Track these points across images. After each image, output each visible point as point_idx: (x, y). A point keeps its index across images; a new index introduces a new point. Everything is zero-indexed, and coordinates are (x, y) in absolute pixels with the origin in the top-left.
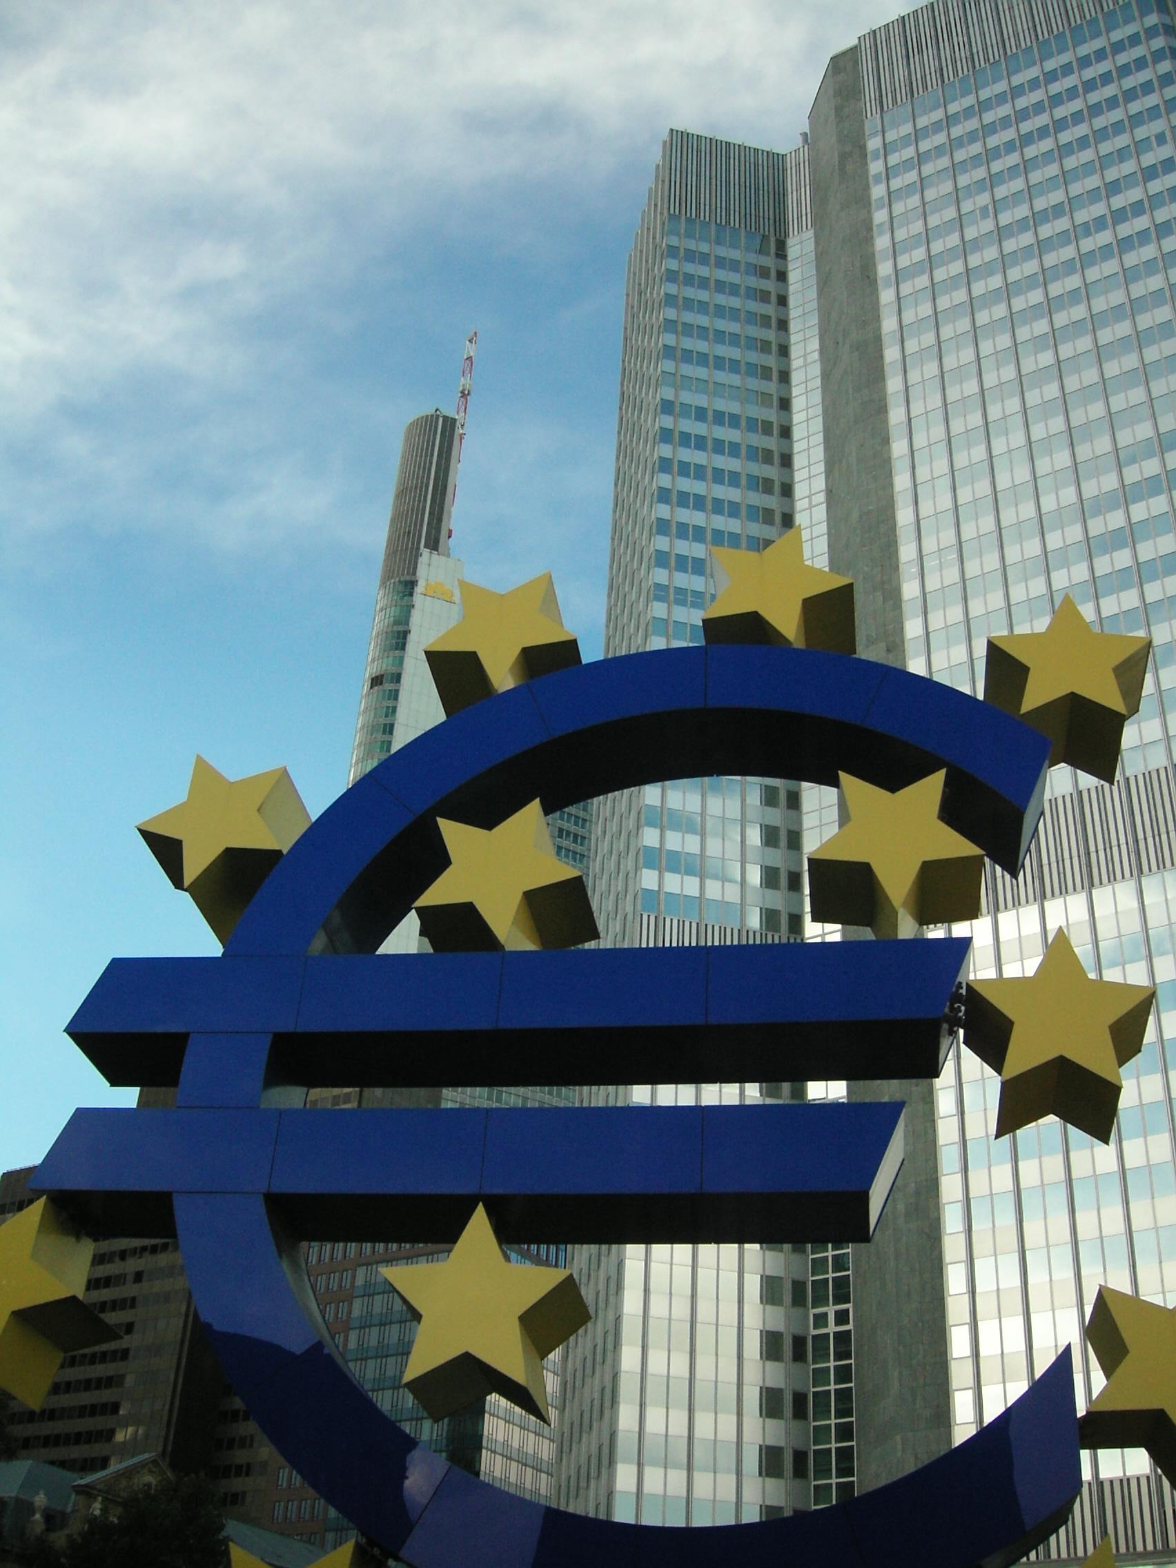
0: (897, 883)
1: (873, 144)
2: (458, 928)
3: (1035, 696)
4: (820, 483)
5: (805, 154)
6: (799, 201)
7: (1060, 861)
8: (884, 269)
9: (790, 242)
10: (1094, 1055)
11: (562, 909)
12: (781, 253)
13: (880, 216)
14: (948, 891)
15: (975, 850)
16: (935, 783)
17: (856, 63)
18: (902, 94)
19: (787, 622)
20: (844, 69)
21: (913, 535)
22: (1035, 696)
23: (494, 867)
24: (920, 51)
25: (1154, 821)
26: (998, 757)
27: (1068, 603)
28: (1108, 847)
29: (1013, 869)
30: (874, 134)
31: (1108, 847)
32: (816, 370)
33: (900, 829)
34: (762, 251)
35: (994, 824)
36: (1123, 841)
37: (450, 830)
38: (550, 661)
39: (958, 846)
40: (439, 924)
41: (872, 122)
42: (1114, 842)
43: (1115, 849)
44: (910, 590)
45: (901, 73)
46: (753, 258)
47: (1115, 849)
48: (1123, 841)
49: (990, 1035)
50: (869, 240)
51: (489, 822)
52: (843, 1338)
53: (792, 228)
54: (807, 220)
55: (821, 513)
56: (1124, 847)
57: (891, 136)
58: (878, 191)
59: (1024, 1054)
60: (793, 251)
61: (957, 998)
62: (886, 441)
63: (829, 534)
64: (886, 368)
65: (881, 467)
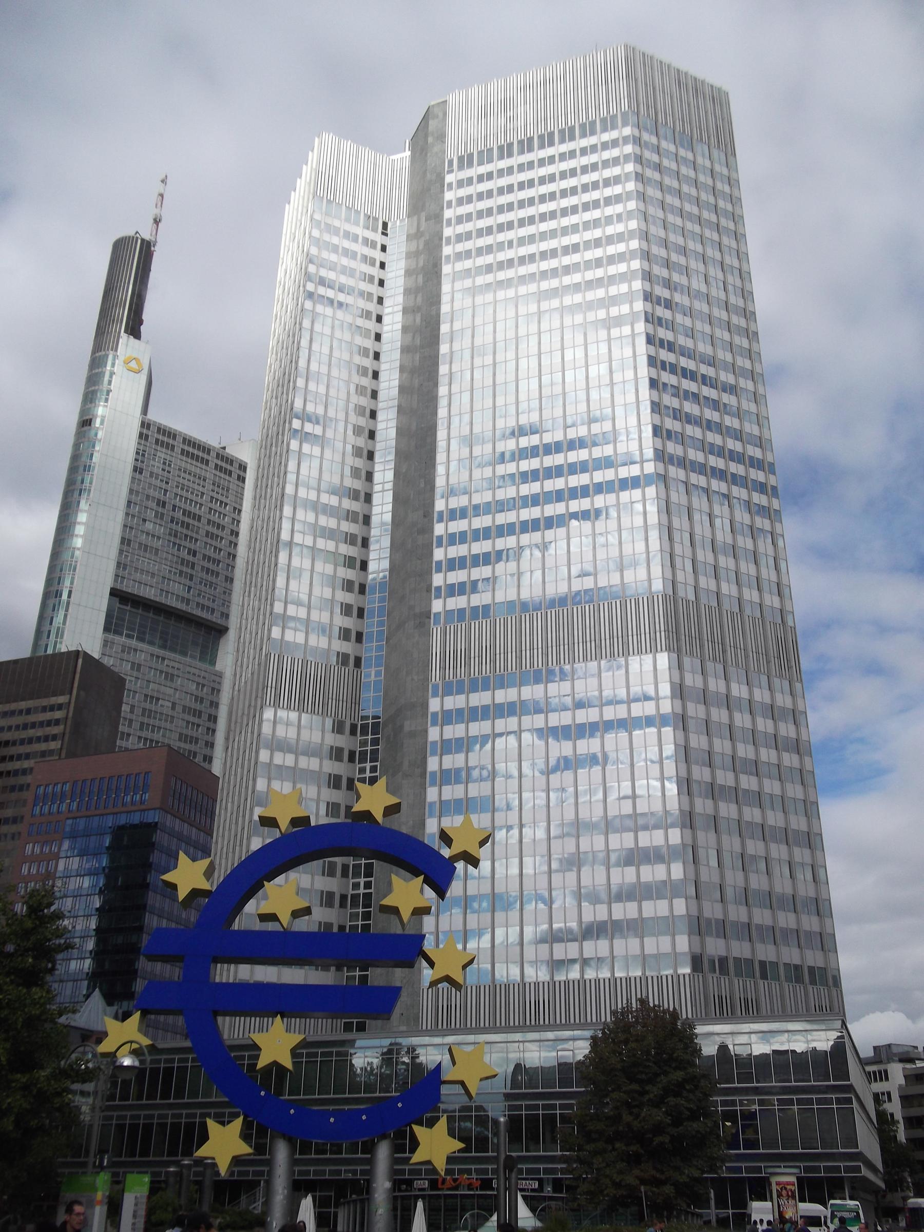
1: (449, 178)
19: (378, 816)
36: (540, 646)
42: (535, 647)
43: (535, 651)
47: (535, 651)
48: (540, 646)
52: (368, 896)
56: (540, 650)
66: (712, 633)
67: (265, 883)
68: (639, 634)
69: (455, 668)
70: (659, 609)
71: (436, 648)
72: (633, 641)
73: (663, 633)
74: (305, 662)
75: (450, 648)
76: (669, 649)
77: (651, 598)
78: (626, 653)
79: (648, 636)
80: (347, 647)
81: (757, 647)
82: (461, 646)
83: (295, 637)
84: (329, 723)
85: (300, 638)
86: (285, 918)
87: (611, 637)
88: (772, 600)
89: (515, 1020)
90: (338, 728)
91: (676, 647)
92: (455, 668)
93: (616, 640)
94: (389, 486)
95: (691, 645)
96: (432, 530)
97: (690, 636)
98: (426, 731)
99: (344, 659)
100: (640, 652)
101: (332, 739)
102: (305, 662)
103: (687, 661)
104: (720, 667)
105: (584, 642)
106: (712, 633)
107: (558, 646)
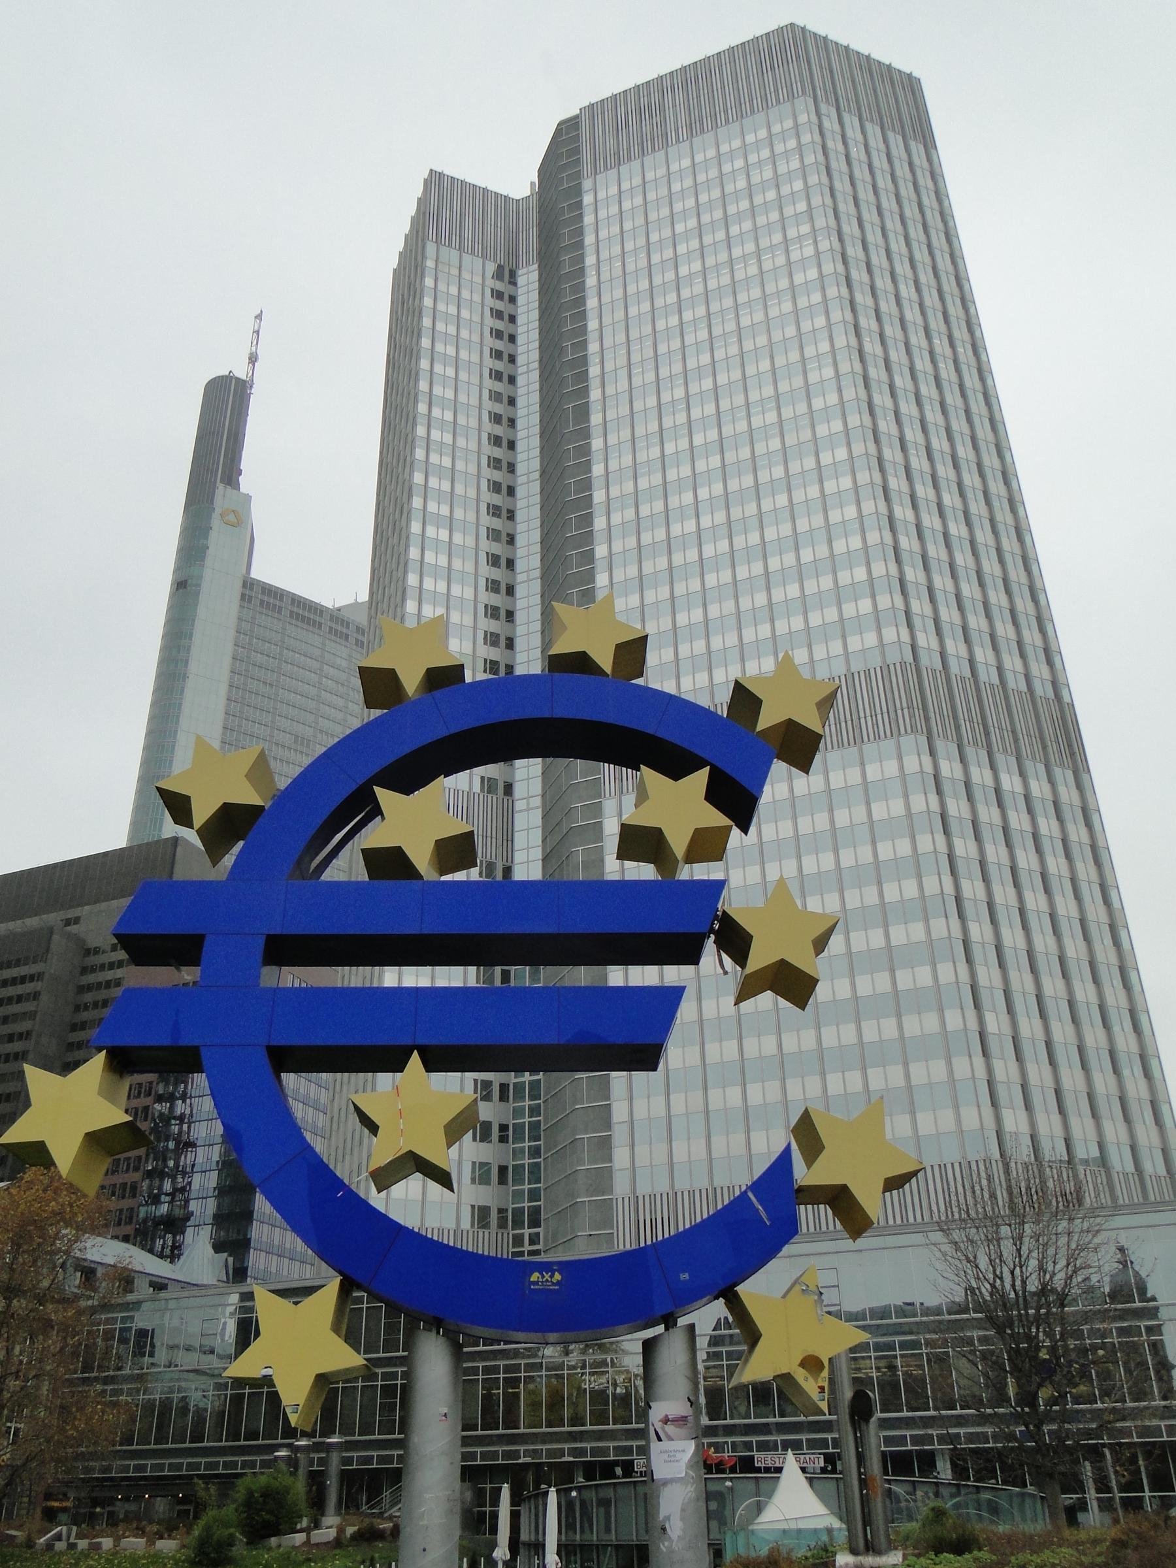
0: (679, 844)
1: (588, 199)
2: (389, 864)
3: (767, 719)
4: (536, 464)
5: (534, 203)
9: (520, 272)
10: (802, 959)
11: (456, 850)
14: (708, 845)
15: (724, 821)
16: (703, 775)
19: (605, 660)
22: (767, 719)
23: (411, 822)
26: (734, 755)
27: (788, 659)
29: (745, 829)
33: (679, 805)
35: (736, 801)
37: (381, 793)
38: (443, 678)
39: (716, 818)
40: (370, 856)
45: (611, 143)
49: (735, 941)
51: (408, 790)
53: (523, 259)
55: (536, 487)
59: (758, 959)
60: (521, 281)
61: (716, 917)
66: (969, 710)
67: (383, 795)
72: (867, 724)
73: (906, 711)
77: (886, 669)
79: (886, 715)
86: (421, 858)
88: (1039, 670)
93: (843, 724)
95: (944, 725)
97: (942, 715)
98: (602, 860)
100: (877, 737)
103: (940, 744)
104: (983, 754)
106: (969, 710)
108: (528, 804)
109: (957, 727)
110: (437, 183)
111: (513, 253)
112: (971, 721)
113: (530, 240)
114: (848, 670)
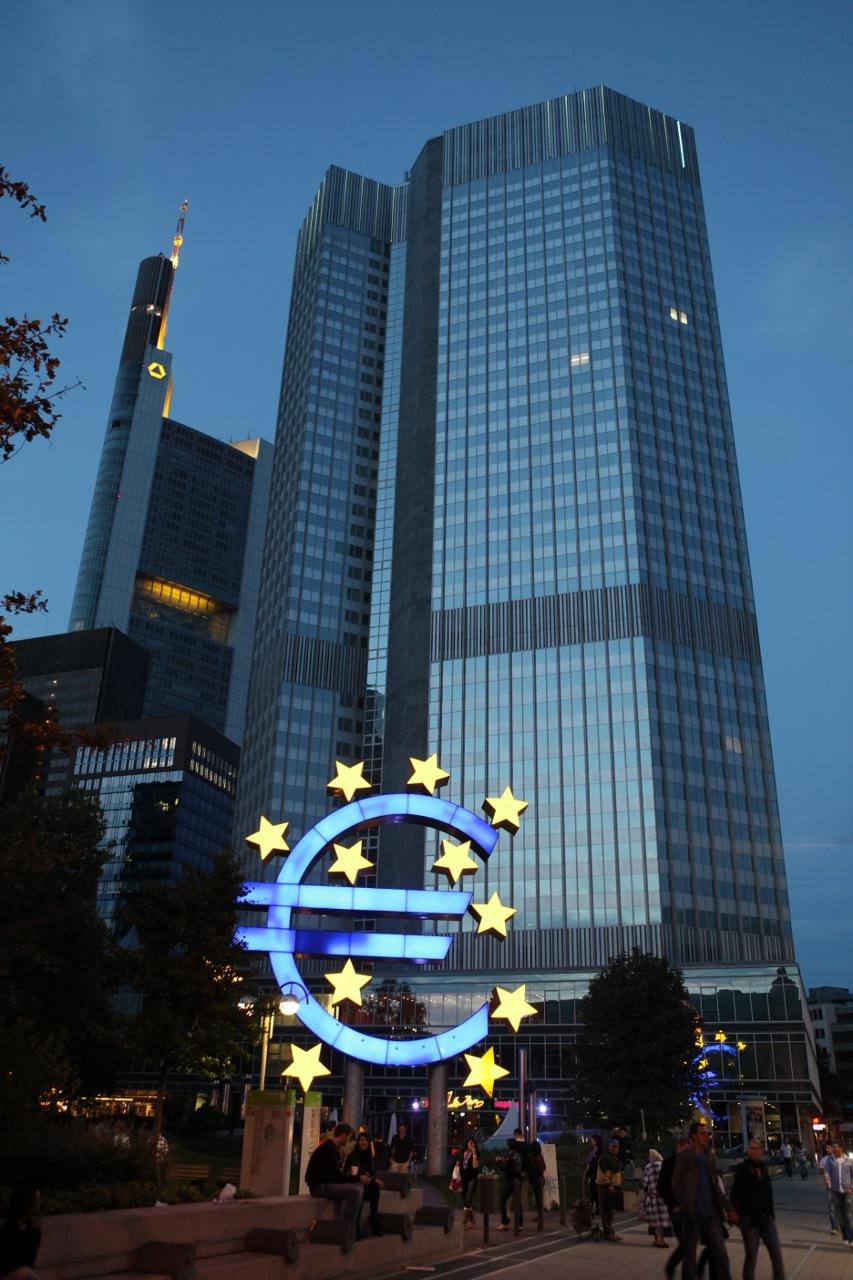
1: (446, 205)
4: (397, 400)
5: (406, 192)
6: (399, 223)
7: (498, 635)
8: (444, 287)
9: (393, 247)
12: (387, 254)
13: (445, 254)
17: (441, 148)
18: (465, 177)
20: (434, 147)
21: (443, 449)
24: (478, 151)
25: (545, 624)
28: (522, 632)
30: (446, 199)
31: (522, 632)
32: (400, 330)
34: (378, 252)
41: (446, 193)
44: (439, 479)
45: (465, 163)
46: (371, 255)
50: (437, 268)
54: (403, 234)
55: (395, 417)
57: (456, 203)
58: (445, 237)
60: (394, 254)
62: (434, 392)
63: (399, 429)
64: (439, 348)
65: (430, 407)
68: (618, 619)
69: (453, 648)
70: (636, 597)
71: (436, 631)
72: (613, 626)
73: (639, 620)
74: (318, 642)
75: (448, 630)
76: (645, 634)
78: (607, 637)
80: (354, 629)
81: (722, 633)
82: (459, 629)
83: (309, 619)
84: (338, 695)
85: (314, 620)
87: (593, 622)
88: (735, 589)
89: (505, 963)
90: (346, 701)
91: (650, 635)
92: (453, 648)
94: (393, 483)
96: (431, 523)
99: (350, 639)
100: (619, 637)
101: (340, 711)
102: (318, 642)
103: (660, 645)
105: (569, 626)
107: (545, 629)
108: (378, 654)
109: (673, 631)
110: (335, 174)
111: (387, 232)
112: (683, 627)
113: (399, 223)
114: (604, 585)
